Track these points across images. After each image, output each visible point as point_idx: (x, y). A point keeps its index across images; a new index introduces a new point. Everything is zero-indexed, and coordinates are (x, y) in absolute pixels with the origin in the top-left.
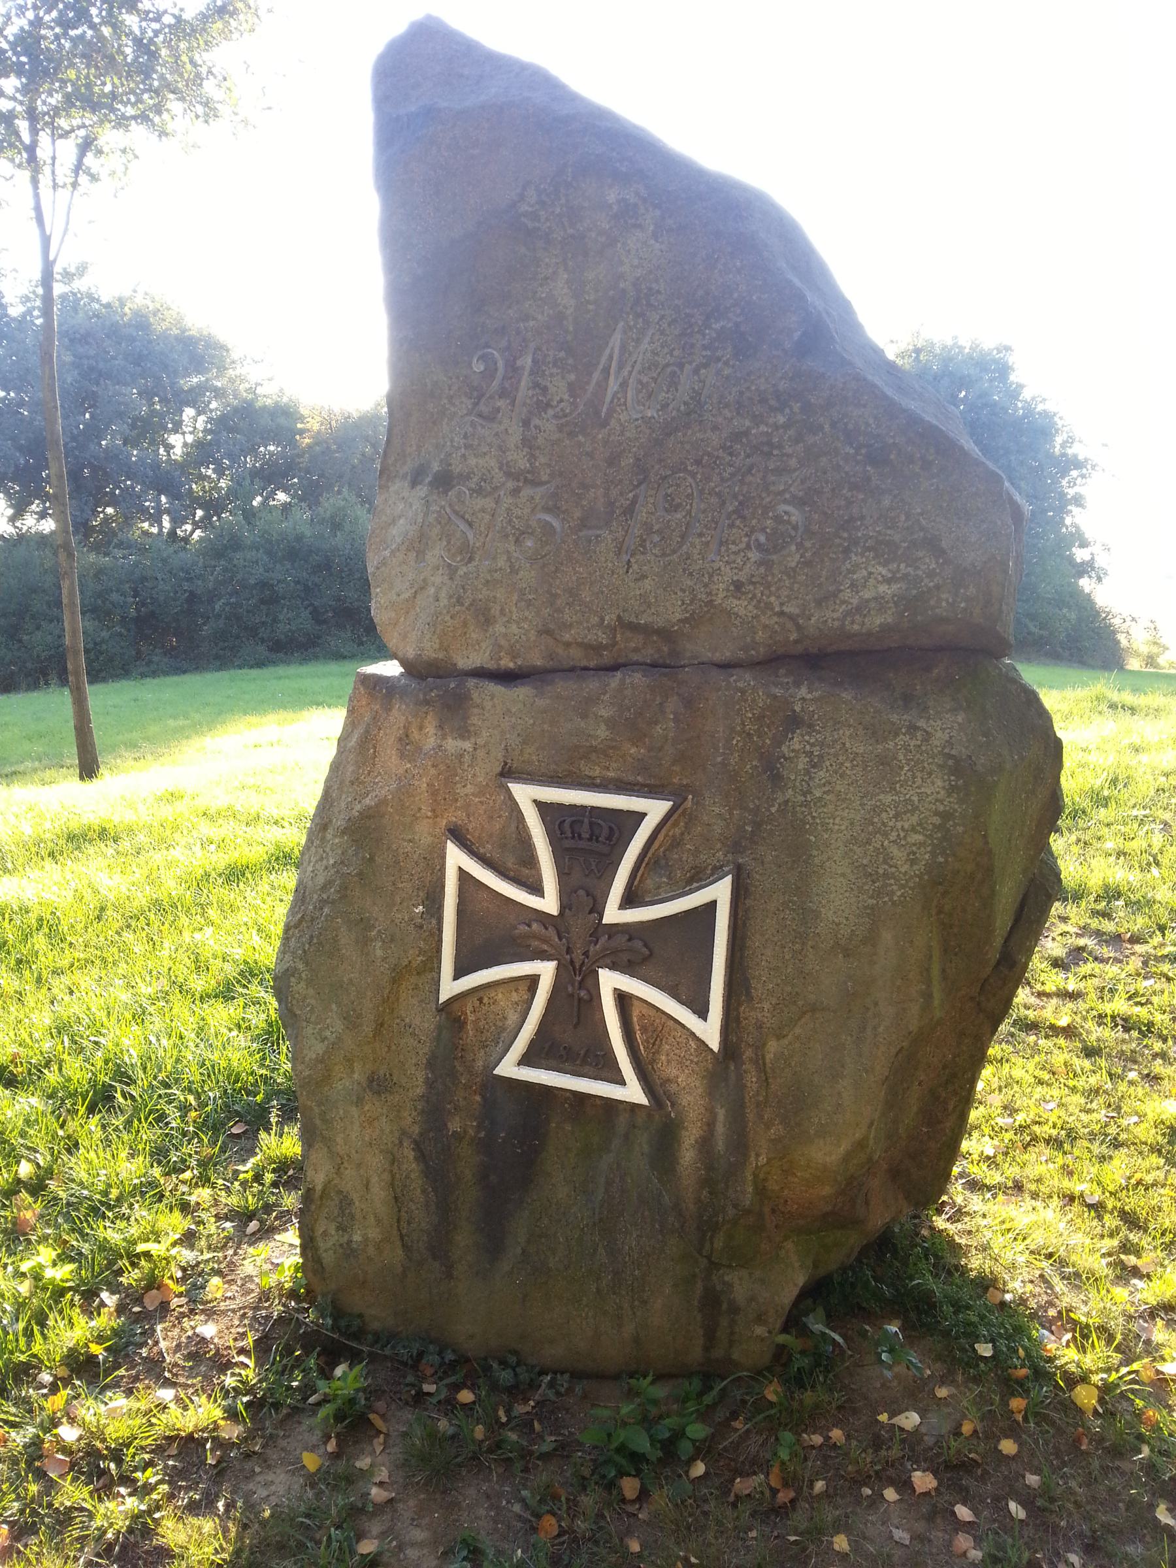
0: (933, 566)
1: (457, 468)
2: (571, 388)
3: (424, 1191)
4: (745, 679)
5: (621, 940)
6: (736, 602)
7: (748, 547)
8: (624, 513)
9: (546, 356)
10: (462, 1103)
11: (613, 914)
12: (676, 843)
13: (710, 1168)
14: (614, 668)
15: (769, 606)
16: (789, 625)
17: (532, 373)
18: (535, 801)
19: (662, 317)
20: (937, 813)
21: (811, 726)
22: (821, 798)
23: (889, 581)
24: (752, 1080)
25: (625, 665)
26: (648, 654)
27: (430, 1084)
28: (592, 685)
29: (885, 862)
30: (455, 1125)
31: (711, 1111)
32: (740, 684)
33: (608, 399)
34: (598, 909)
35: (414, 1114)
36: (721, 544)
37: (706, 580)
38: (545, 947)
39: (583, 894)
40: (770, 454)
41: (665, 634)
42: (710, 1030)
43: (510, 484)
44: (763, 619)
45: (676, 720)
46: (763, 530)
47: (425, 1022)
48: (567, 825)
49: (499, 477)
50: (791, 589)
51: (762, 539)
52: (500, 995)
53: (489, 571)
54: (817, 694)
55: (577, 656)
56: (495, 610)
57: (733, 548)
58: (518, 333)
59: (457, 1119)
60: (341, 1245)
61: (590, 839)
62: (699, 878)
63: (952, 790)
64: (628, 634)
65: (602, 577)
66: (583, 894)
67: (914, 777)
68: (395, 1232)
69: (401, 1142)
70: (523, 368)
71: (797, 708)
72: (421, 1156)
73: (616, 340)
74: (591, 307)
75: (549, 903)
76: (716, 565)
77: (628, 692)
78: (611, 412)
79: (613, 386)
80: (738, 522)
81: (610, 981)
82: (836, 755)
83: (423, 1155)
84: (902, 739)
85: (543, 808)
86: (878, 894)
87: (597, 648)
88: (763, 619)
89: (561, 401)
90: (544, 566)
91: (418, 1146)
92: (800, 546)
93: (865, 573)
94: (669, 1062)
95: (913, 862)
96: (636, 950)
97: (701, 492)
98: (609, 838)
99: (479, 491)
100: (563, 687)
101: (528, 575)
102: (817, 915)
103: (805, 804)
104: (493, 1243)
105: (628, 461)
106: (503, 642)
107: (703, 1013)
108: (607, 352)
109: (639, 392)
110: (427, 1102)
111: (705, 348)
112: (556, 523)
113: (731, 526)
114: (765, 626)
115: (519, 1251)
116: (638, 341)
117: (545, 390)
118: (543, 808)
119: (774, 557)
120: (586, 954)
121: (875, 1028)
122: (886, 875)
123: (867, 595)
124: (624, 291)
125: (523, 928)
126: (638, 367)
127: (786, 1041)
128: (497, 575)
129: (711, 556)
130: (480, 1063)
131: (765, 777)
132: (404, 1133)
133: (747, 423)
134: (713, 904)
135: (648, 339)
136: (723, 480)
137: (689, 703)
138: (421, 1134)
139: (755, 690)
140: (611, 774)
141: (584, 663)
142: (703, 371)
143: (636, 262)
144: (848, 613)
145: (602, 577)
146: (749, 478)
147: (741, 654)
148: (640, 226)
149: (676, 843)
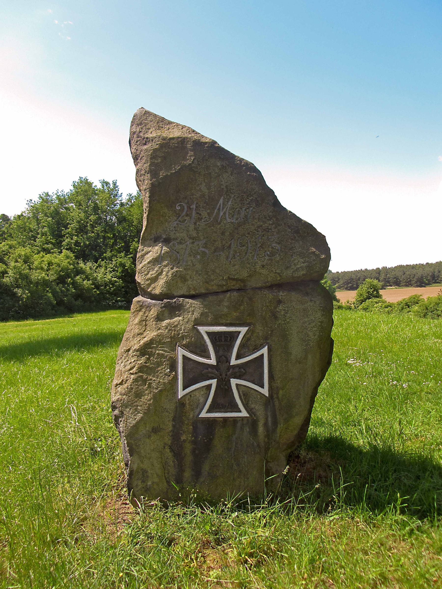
0: (314, 258)
1: (172, 236)
2: (208, 214)
3: (173, 462)
4: (266, 292)
5: (237, 370)
6: (262, 271)
7: (265, 256)
8: (228, 248)
9: (200, 205)
10: (186, 430)
11: (233, 362)
12: (249, 339)
13: (268, 431)
14: (227, 291)
15: (272, 271)
16: (278, 276)
17: (196, 210)
18: (206, 332)
19: (235, 196)
20: (319, 322)
21: (284, 302)
22: (289, 322)
23: (303, 263)
24: (277, 403)
25: (230, 290)
26: (237, 286)
27: (174, 426)
28: (221, 296)
29: (308, 336)
30: (183, 437)
31: (266, 414)
32: (265, 293)
33: (220, 217)
34: (228, 361)
35: (169, 437)
36: (257, 255)
37: (254, 265)
38: (213, 375)
39: (223, 358)
40: (268, 231)
41: (243, 281)
42: (265, 391)
43: (191, 241)
44: (270, 275)
45: (247, 304)
46: (269, 251)
47: (170, 406)
48: (217, 338)
49: (187, 239)
50: (278, 266)
51: (269, 253)
52: (197, 393)
53: (186, 266)
54: (285, 294)
55: (215, 288)
56: (188, 277)
57: (261, 256)
58: (191, 199)
59: (184, 435)
60: (143, 488)
61: (225, 341)
62: (257, 348)
63: (323, 315)
64: (231, 281)
65: (222, 266)
66: (223, 358)
67: (313, 313)
68: (164, 478)
69: (164, 447)
70: (193, 209)
71: (280, 298)
72: (172, 450)
73: (221, 201)
74: (213, 192)
75: (213, 361)
76: (256, 261)
77: (233, 297)
78: (221, 220)
79: (221, 214)
80: (261, 249)
81: (234, 382)
82: (292, 310)
83: (172, 450)
84: (309, 304)
85: (208, 334)
86: (307, 345)
87: (222, 286)
88: (270, 275)
89: (206, 217)
90: (204, 263)
91: (170, 448)
92: (279, 255)
93: (297, 261)
94: (252, 403)
95: (315, 336)
96: (240, 372)
97: (250, 242)
98: (230, 340)
99: (180, 243)
100: (211, 298)
101: (199, 266)
102: (291, 354)
103: (285, 324)
104: (197, 473)
105: (227, 234)
106: (191, 286)
107: (262, 387)
108: (219, 205)
109: (229, 215)
110: (173, 432)
111: (248, 204)
112: (207, 251)
113: (260, 250)
114: (271, 276)
115: (206, 473)
116: (228, 202)
117: (200, 214)
118: (208, 334)
119: (273, 258)
120: (226, 375)
121: (308, 382)
122: (309, 340)
123: (298, 266)
124: (223, 189)
125: (206, 371)
126: (228, 209)
127: (284, 391)
128: (188, 267)
129: (255, 258)
130: (191, 416)
131: (273, 317)
132: (165, 444)
133: (262, 223)
134: (263, 355)
135: (231, 201)
136: (256, 238)
137: (250, 299)
138: (171, 443)
139: (270, 295)
140: (228, 322)
141: (218, 291)
142: (247, 210)
143: (226, 181)
144: (294, 271)
145: (222, 266)
146: (263, 238)
147: (264, 285)
148: (227, 172)
149: (249, 339)
